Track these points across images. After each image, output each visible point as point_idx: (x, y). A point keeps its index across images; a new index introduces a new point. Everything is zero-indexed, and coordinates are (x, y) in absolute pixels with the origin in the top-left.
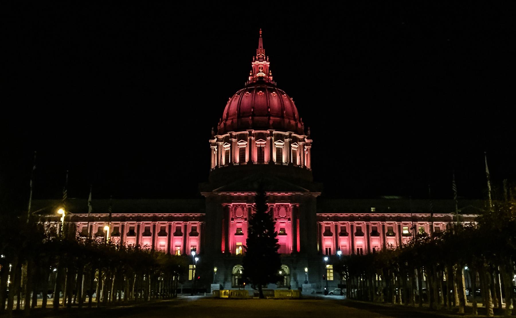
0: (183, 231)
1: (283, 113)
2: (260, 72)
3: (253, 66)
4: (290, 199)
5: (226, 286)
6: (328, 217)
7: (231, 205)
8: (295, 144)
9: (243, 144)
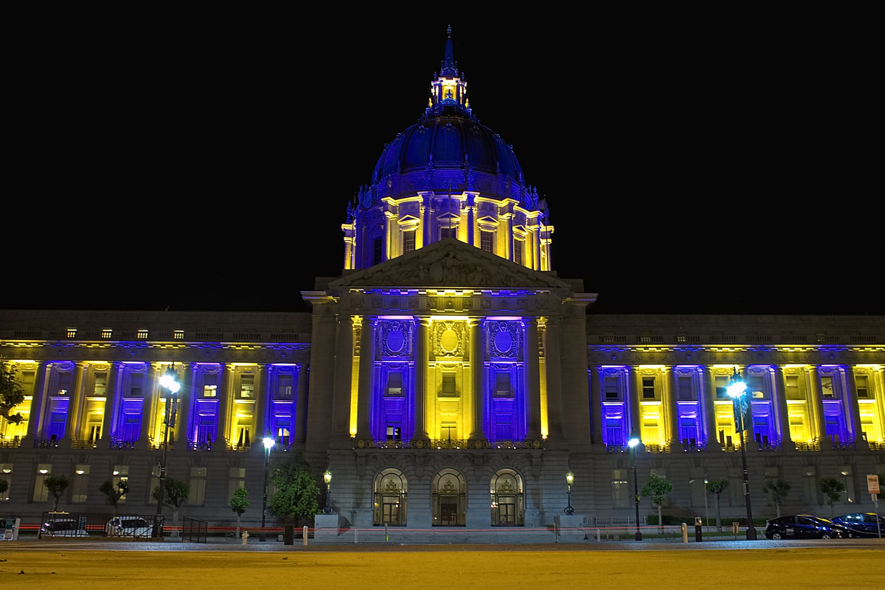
5: (357, 523)
8: (520, 228)
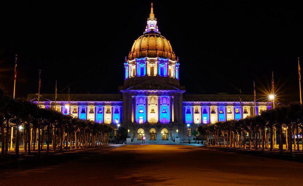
0: (111, 111)
1: (164, 49)
2: (151, 26)
3: (147, 23)
4: (169, 94)
5: (134, 140)
6: (189, 103)
7: (137, 97)
8: (171, 66)
9: (143, 65)
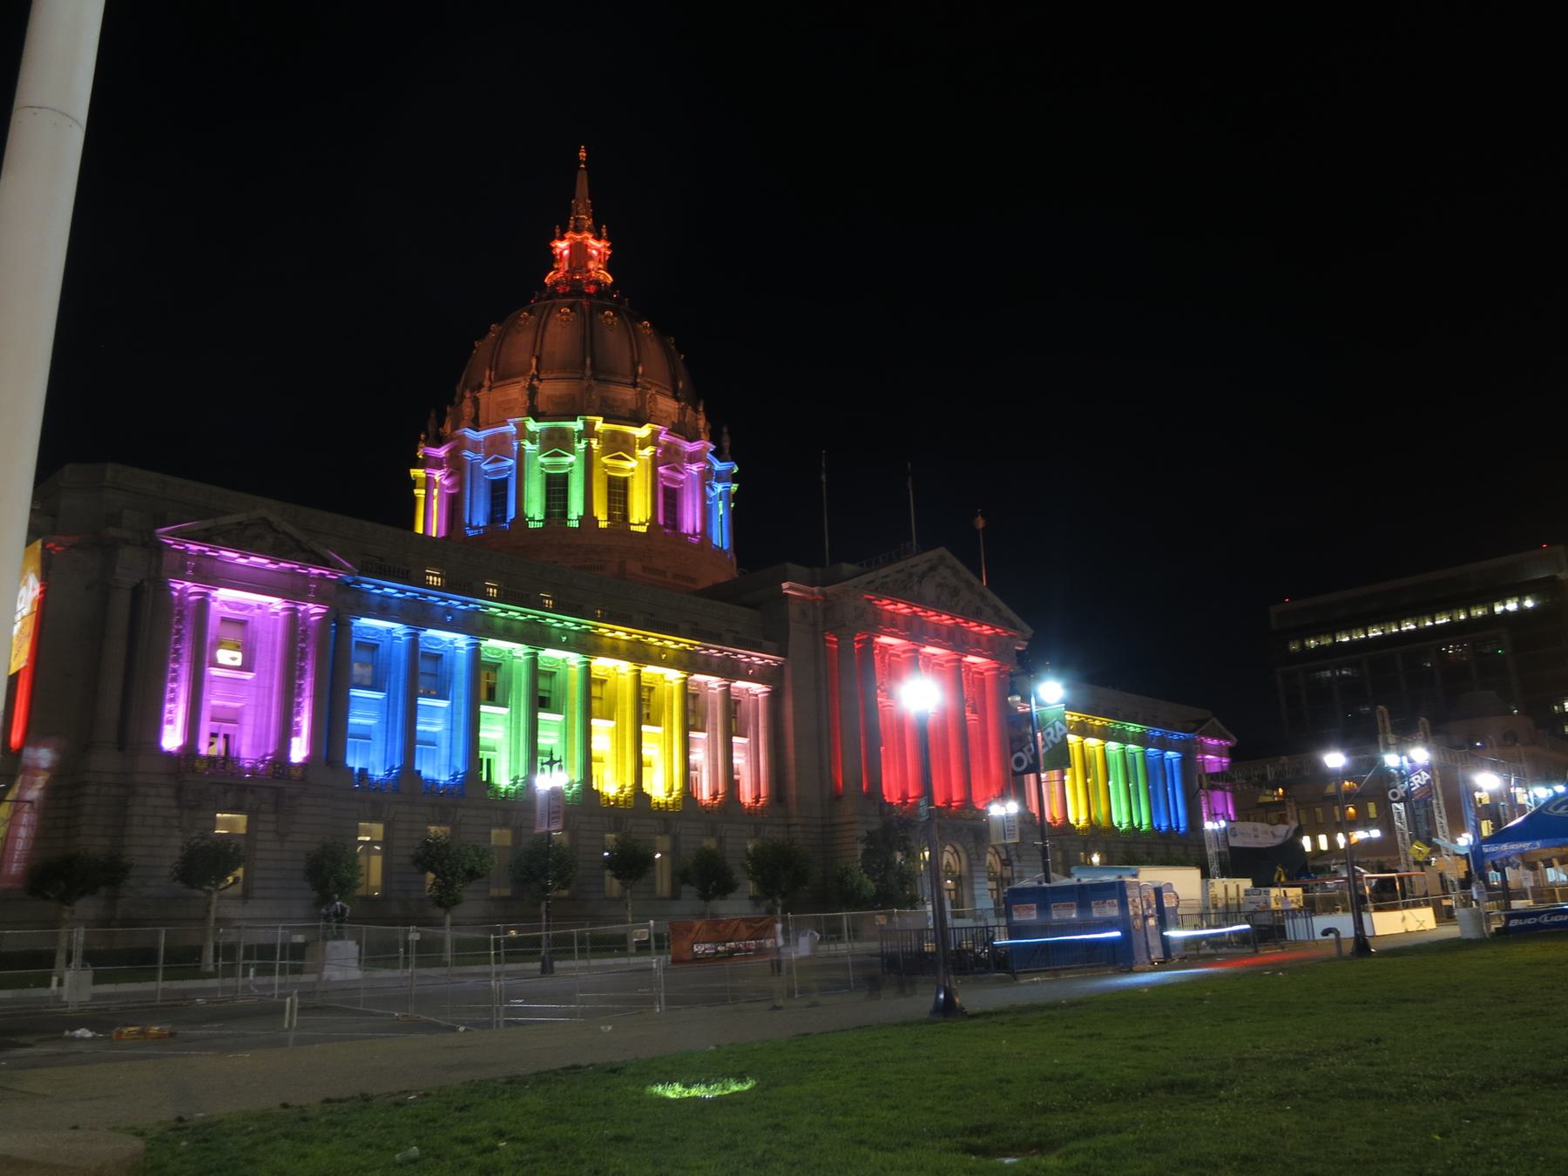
8: (674, 469)
